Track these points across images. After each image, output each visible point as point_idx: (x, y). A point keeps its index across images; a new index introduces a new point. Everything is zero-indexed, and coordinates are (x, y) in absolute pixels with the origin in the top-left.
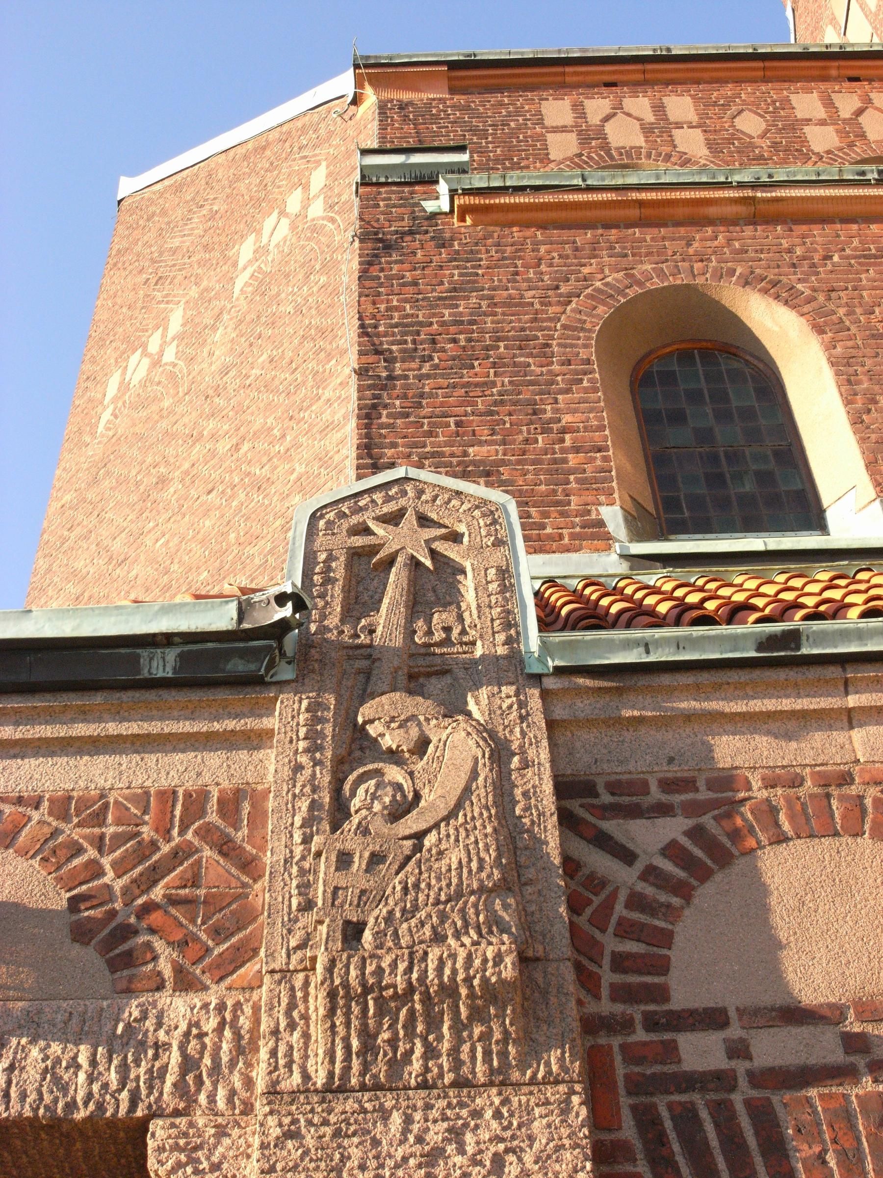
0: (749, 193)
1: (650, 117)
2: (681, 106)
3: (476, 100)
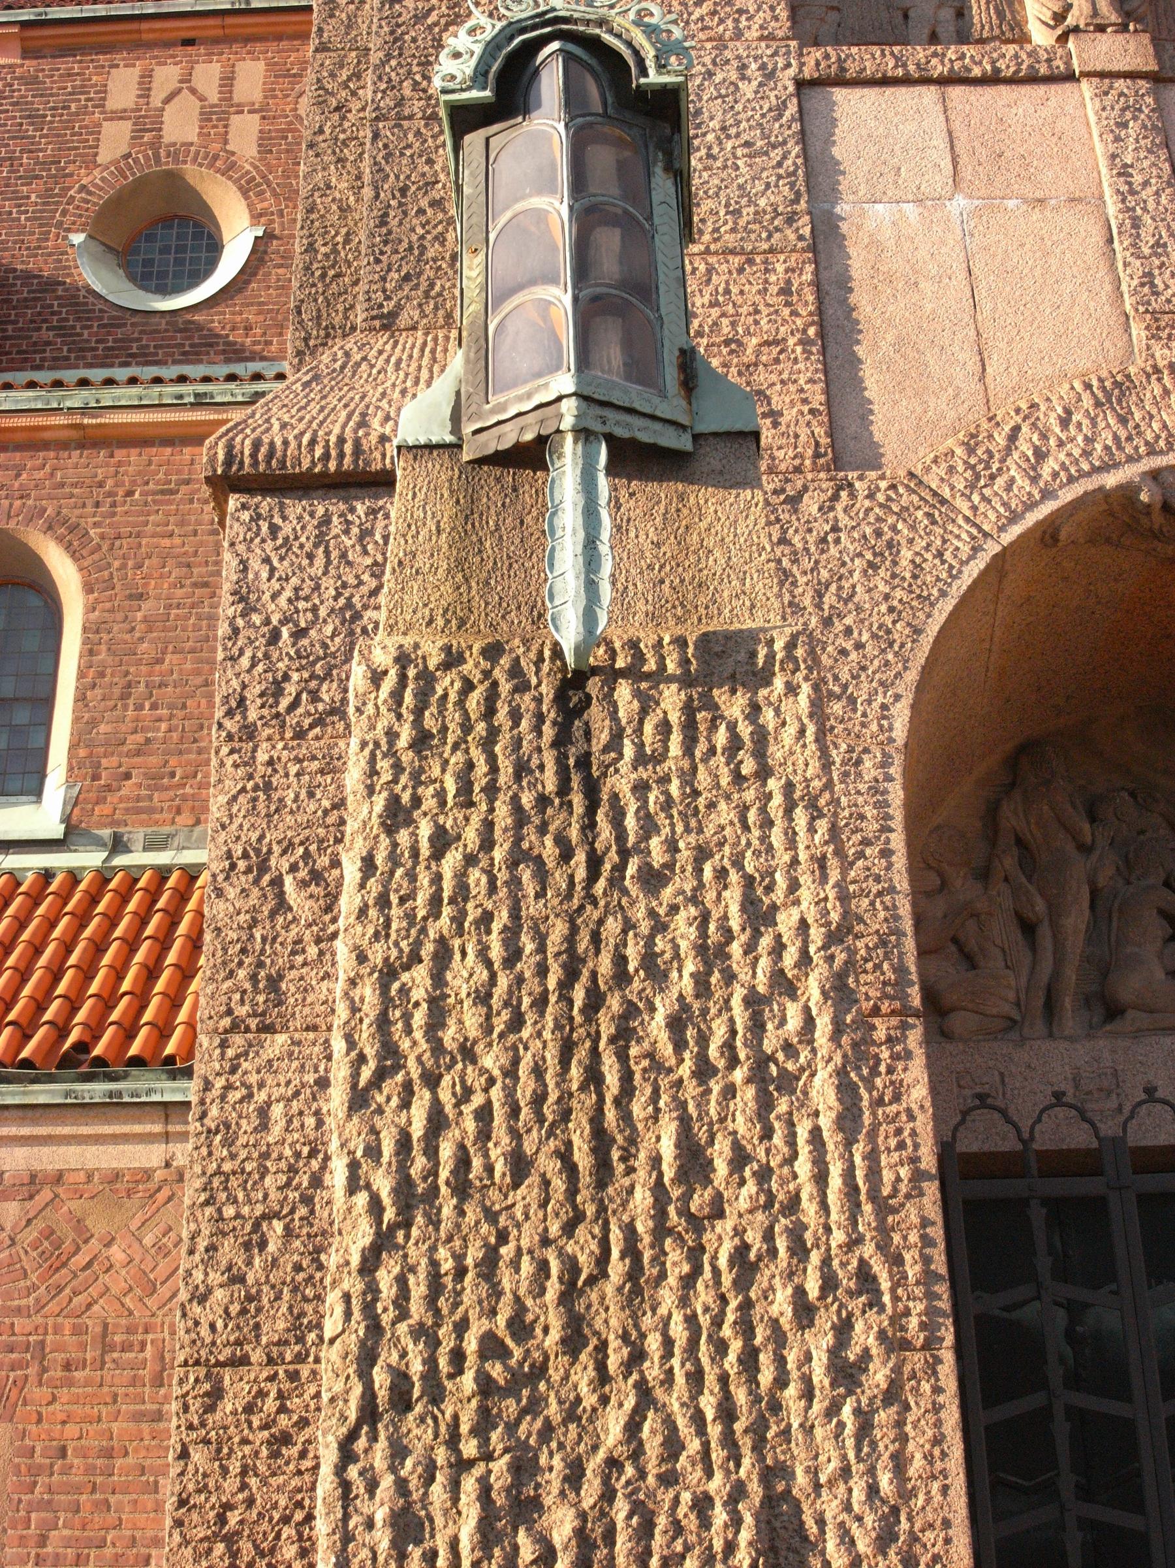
0: (77, 419)
1: (214, 97)
2: (252, 75)
3: (46, 64)
